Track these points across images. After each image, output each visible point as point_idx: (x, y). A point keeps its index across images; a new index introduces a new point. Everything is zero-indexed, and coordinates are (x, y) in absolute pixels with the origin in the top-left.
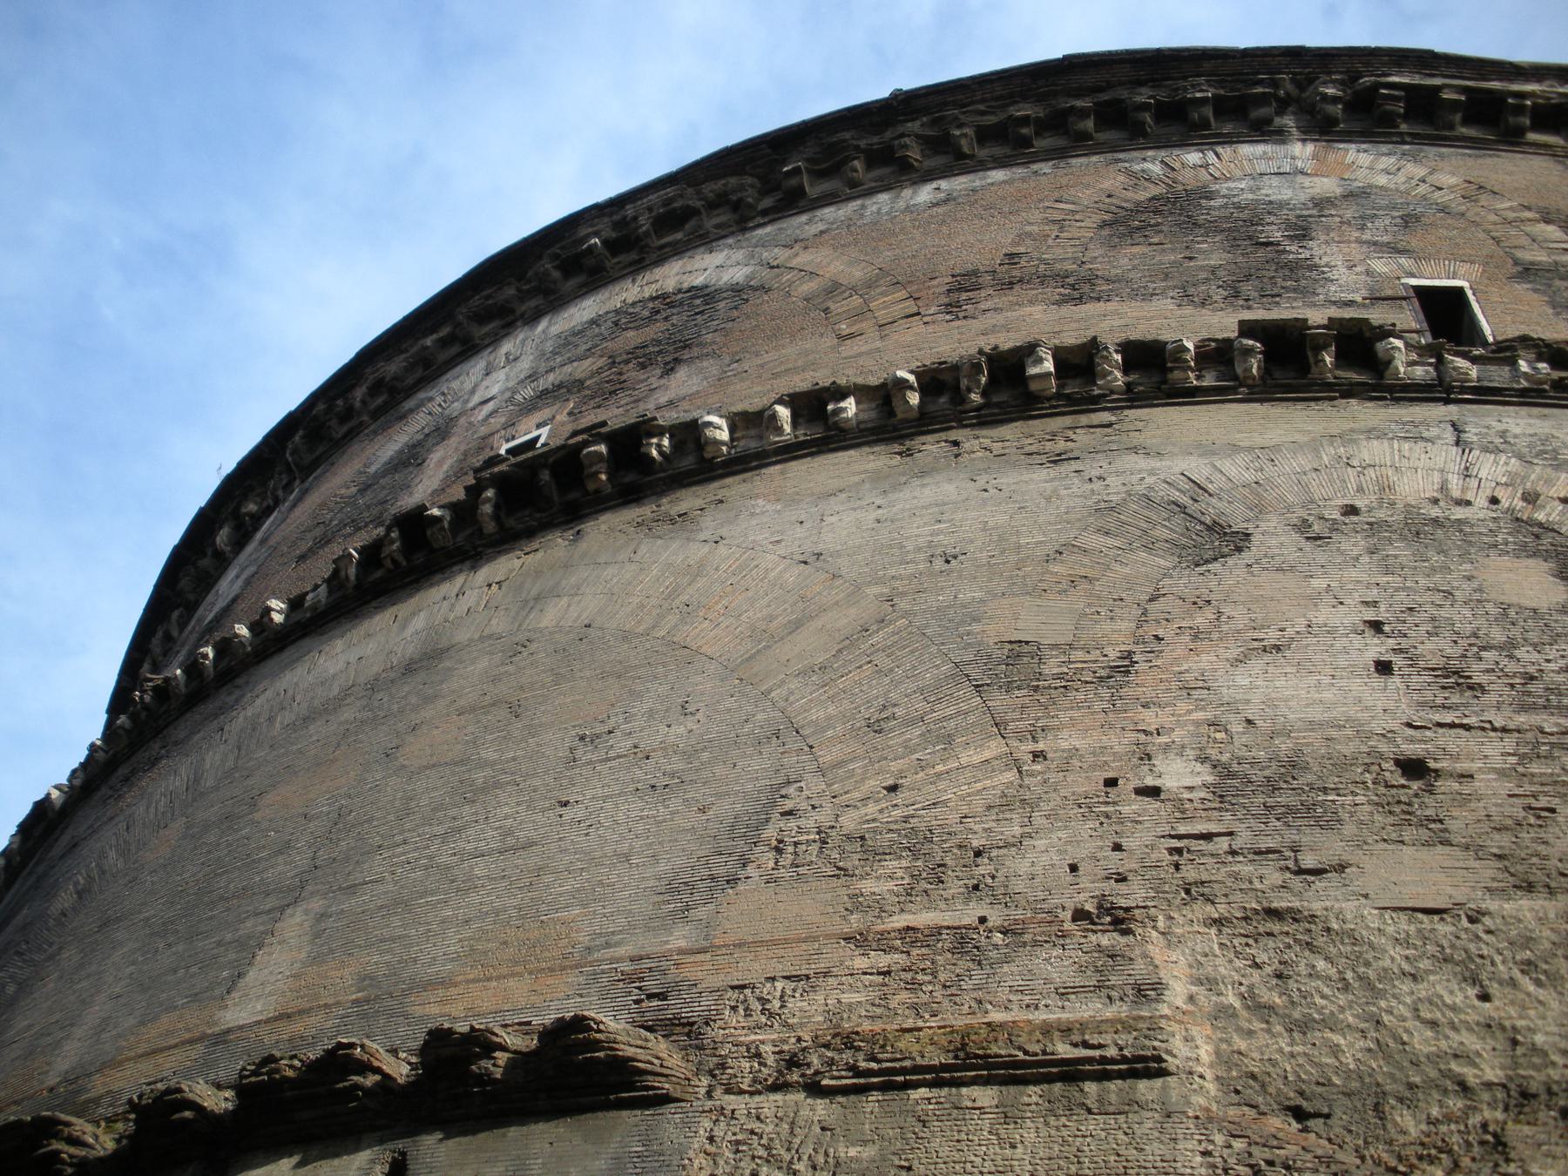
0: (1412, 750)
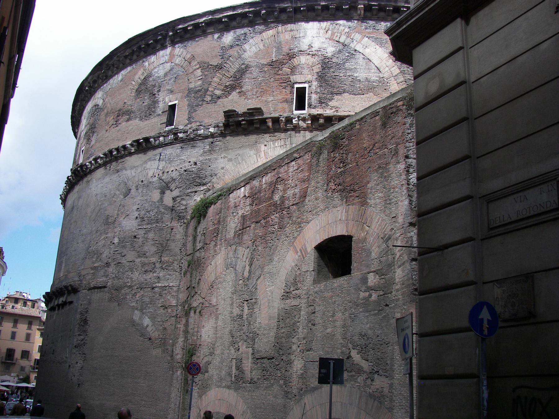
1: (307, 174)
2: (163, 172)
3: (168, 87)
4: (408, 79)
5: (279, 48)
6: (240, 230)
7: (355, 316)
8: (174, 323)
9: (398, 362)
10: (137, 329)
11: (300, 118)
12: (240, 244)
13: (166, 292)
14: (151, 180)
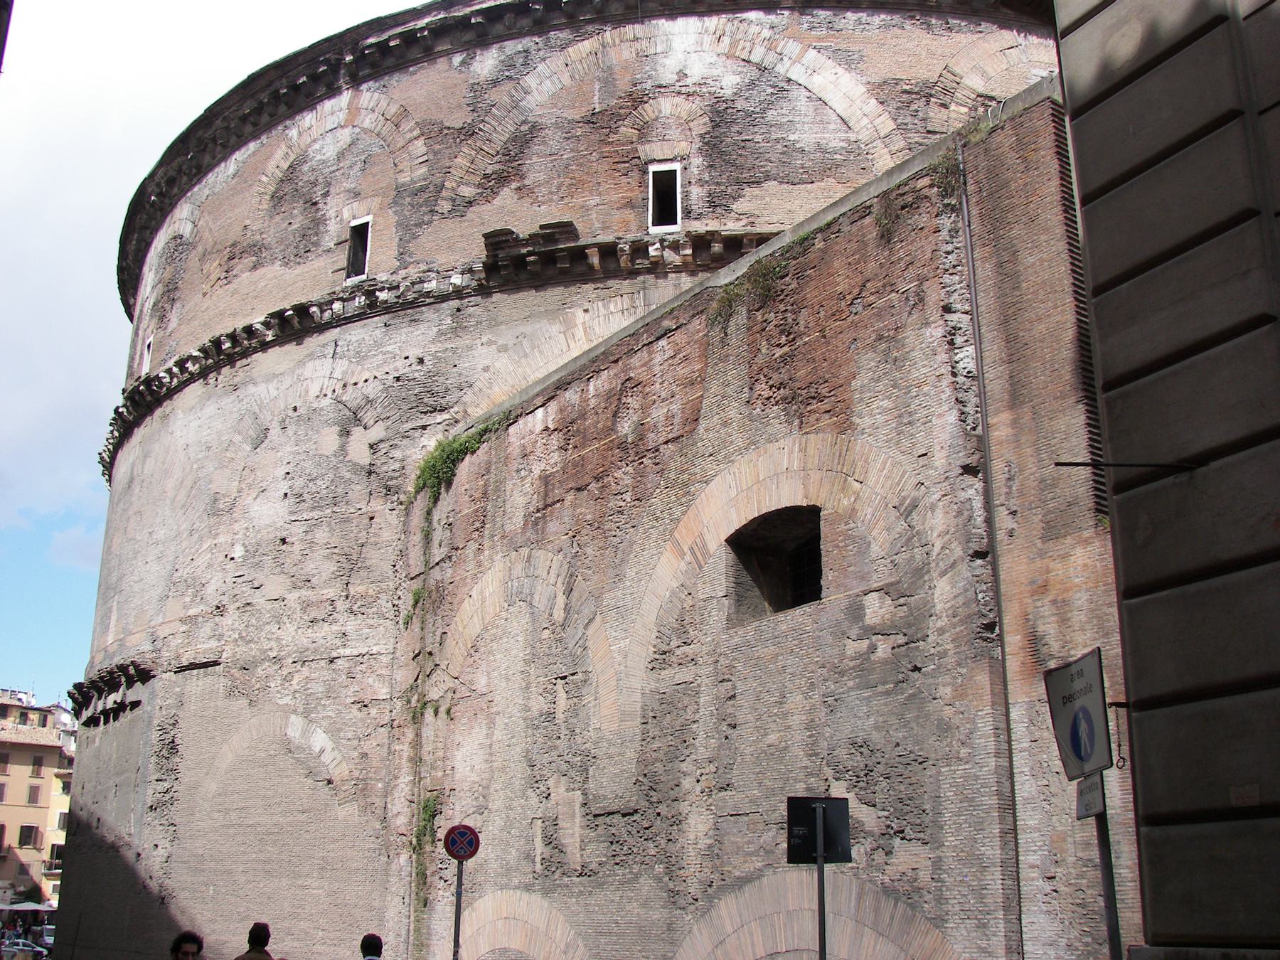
0: (284, 534)
1: (698, 367)
2: (345, 386)
3: (347, 185)
4: (916, 143)
5: (608, 81)
6: (538, 511)
7: (836, 700)
8: (386, 741)
9: (953, 806)
10: (298, 760)
11: (666, 244)
12: (540, 542)
13: (363, 667)
14: (315, 405)
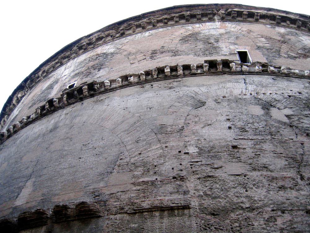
0: (235, 144)
